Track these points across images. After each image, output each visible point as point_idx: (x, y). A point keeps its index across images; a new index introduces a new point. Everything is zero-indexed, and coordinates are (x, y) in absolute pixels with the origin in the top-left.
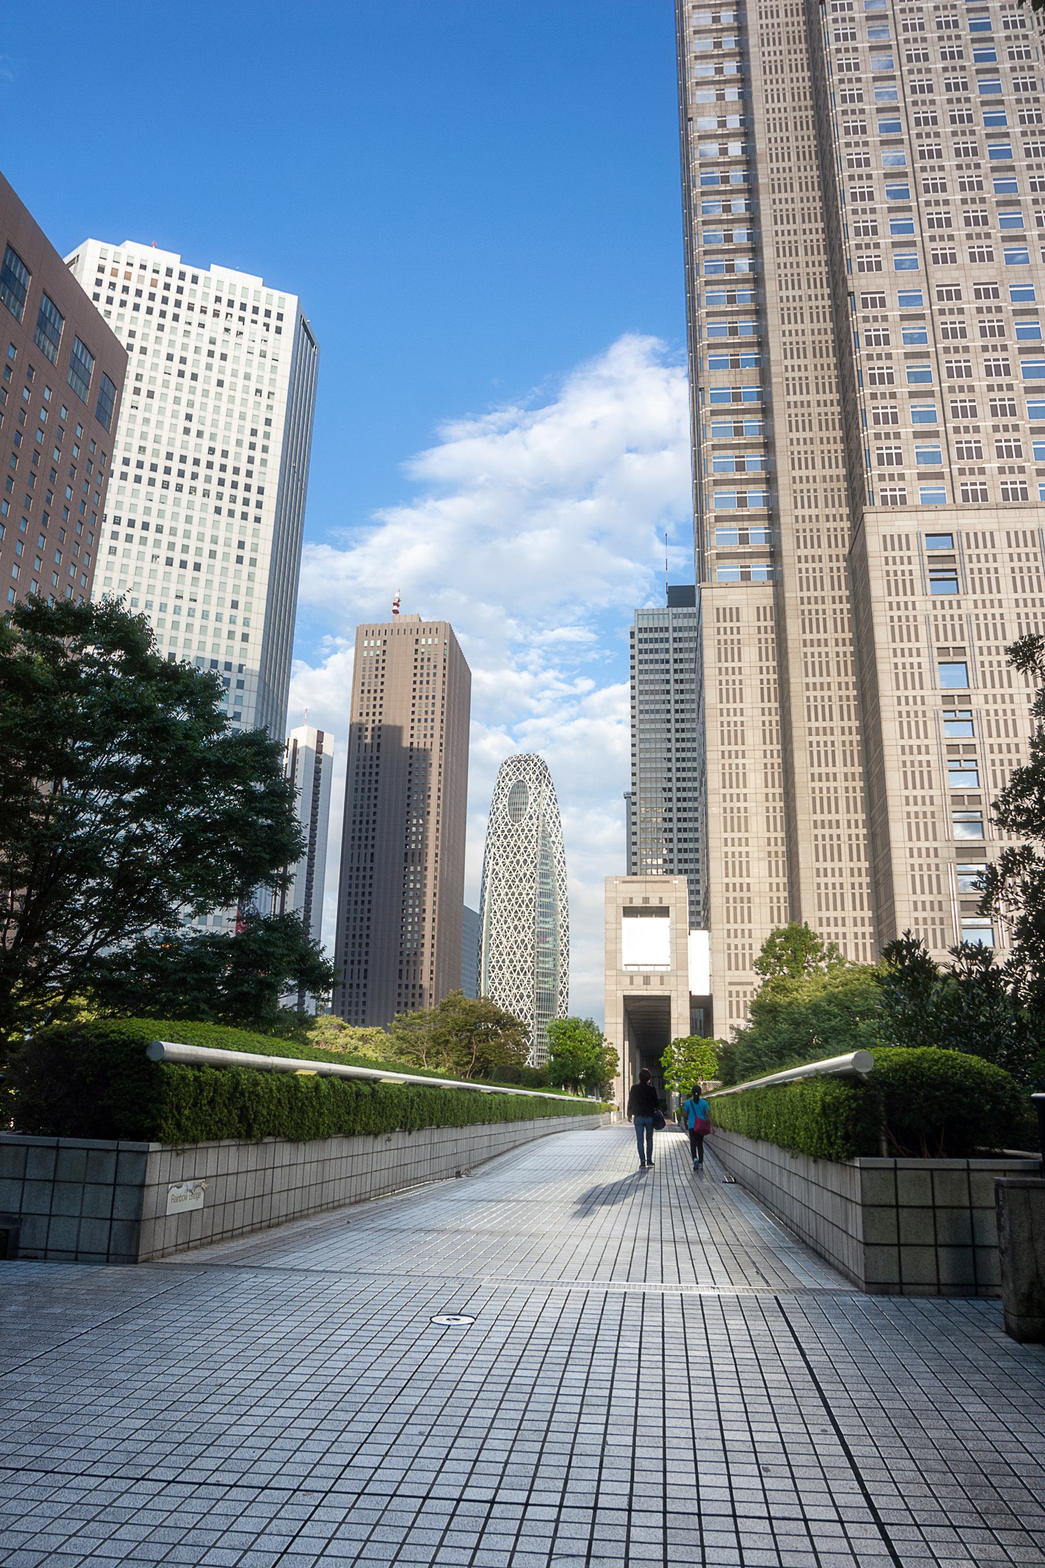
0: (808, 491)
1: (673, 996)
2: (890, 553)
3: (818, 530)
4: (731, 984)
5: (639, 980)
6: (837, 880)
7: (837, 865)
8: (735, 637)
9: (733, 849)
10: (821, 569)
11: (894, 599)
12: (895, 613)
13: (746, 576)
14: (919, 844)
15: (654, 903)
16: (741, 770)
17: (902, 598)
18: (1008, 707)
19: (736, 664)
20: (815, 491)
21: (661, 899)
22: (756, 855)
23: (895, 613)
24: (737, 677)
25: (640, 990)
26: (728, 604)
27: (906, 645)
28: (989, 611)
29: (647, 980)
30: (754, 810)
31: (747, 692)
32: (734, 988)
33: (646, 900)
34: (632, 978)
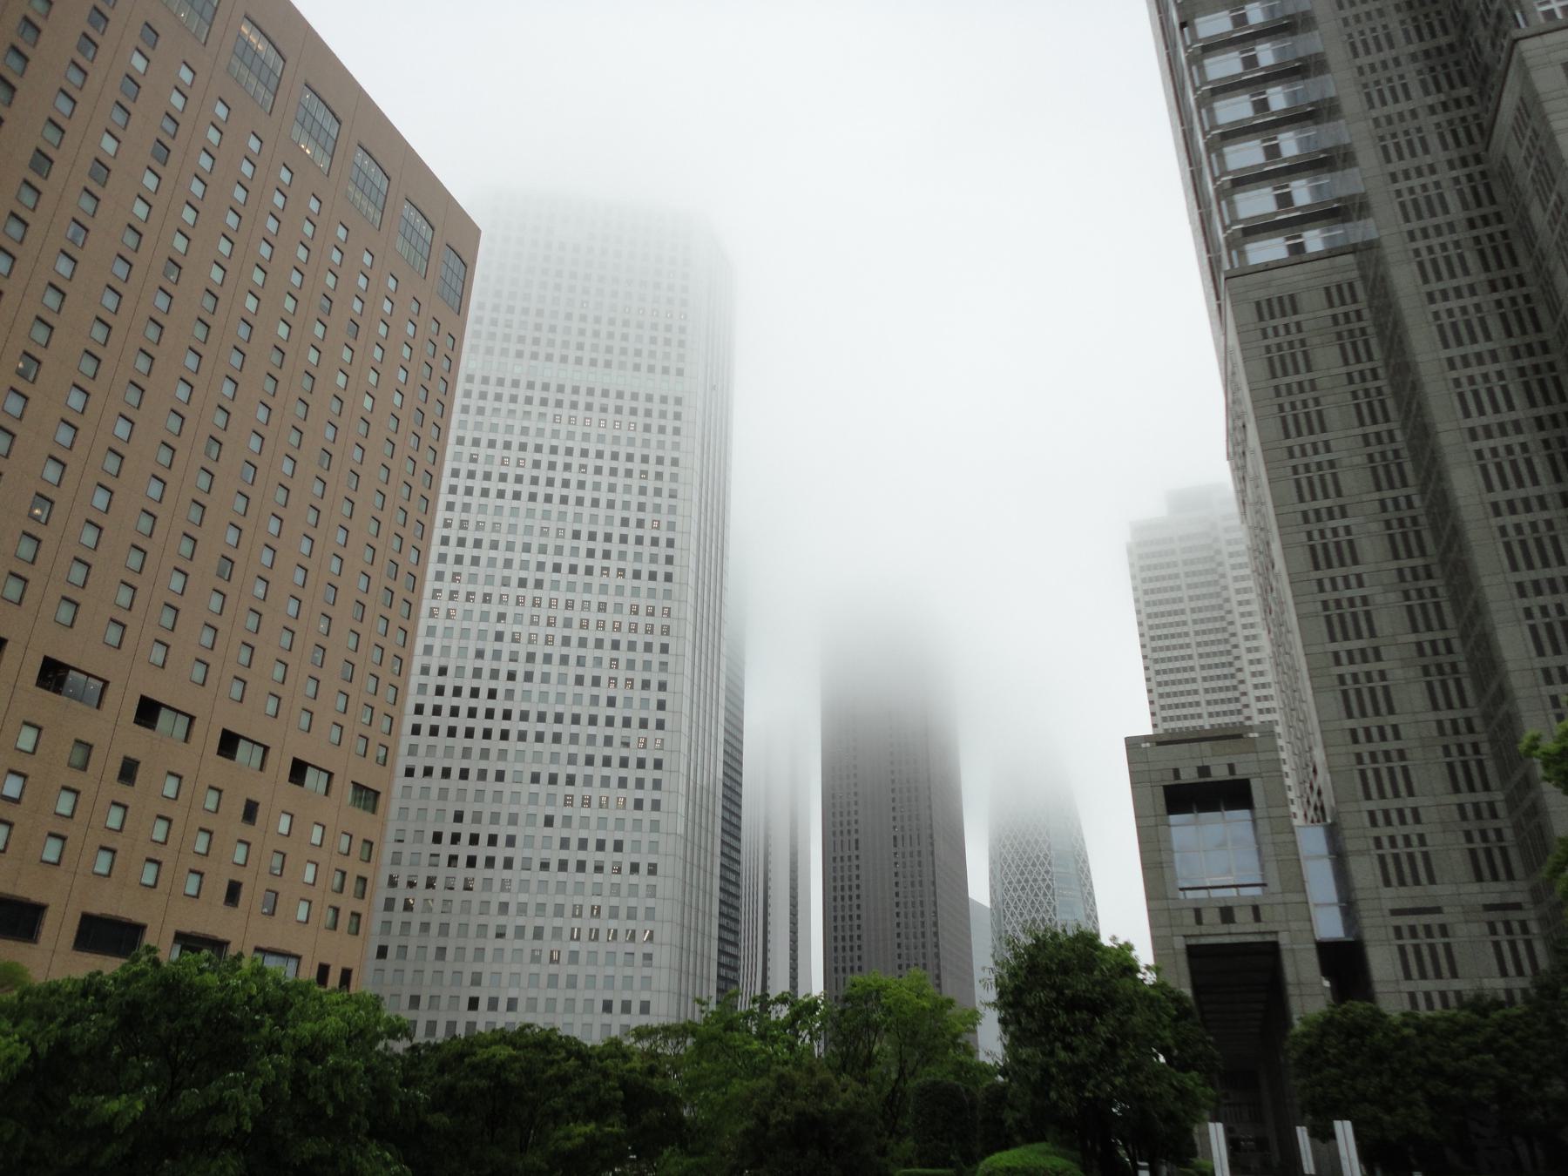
1: (1284, 940)
3: (1419, 130)
4: (1395, 912)
5: (1211, 917)
15: (1219, 773)
16: (1342, 536)
19: (1304, 376)
20: (1401, 77)
21: (1231, 768)
22: (1399, 673)
25: (1216, 933)
26: (1273, 292)
30: (1379, 599)
31: (1332, 416)
33: (1204, 771)
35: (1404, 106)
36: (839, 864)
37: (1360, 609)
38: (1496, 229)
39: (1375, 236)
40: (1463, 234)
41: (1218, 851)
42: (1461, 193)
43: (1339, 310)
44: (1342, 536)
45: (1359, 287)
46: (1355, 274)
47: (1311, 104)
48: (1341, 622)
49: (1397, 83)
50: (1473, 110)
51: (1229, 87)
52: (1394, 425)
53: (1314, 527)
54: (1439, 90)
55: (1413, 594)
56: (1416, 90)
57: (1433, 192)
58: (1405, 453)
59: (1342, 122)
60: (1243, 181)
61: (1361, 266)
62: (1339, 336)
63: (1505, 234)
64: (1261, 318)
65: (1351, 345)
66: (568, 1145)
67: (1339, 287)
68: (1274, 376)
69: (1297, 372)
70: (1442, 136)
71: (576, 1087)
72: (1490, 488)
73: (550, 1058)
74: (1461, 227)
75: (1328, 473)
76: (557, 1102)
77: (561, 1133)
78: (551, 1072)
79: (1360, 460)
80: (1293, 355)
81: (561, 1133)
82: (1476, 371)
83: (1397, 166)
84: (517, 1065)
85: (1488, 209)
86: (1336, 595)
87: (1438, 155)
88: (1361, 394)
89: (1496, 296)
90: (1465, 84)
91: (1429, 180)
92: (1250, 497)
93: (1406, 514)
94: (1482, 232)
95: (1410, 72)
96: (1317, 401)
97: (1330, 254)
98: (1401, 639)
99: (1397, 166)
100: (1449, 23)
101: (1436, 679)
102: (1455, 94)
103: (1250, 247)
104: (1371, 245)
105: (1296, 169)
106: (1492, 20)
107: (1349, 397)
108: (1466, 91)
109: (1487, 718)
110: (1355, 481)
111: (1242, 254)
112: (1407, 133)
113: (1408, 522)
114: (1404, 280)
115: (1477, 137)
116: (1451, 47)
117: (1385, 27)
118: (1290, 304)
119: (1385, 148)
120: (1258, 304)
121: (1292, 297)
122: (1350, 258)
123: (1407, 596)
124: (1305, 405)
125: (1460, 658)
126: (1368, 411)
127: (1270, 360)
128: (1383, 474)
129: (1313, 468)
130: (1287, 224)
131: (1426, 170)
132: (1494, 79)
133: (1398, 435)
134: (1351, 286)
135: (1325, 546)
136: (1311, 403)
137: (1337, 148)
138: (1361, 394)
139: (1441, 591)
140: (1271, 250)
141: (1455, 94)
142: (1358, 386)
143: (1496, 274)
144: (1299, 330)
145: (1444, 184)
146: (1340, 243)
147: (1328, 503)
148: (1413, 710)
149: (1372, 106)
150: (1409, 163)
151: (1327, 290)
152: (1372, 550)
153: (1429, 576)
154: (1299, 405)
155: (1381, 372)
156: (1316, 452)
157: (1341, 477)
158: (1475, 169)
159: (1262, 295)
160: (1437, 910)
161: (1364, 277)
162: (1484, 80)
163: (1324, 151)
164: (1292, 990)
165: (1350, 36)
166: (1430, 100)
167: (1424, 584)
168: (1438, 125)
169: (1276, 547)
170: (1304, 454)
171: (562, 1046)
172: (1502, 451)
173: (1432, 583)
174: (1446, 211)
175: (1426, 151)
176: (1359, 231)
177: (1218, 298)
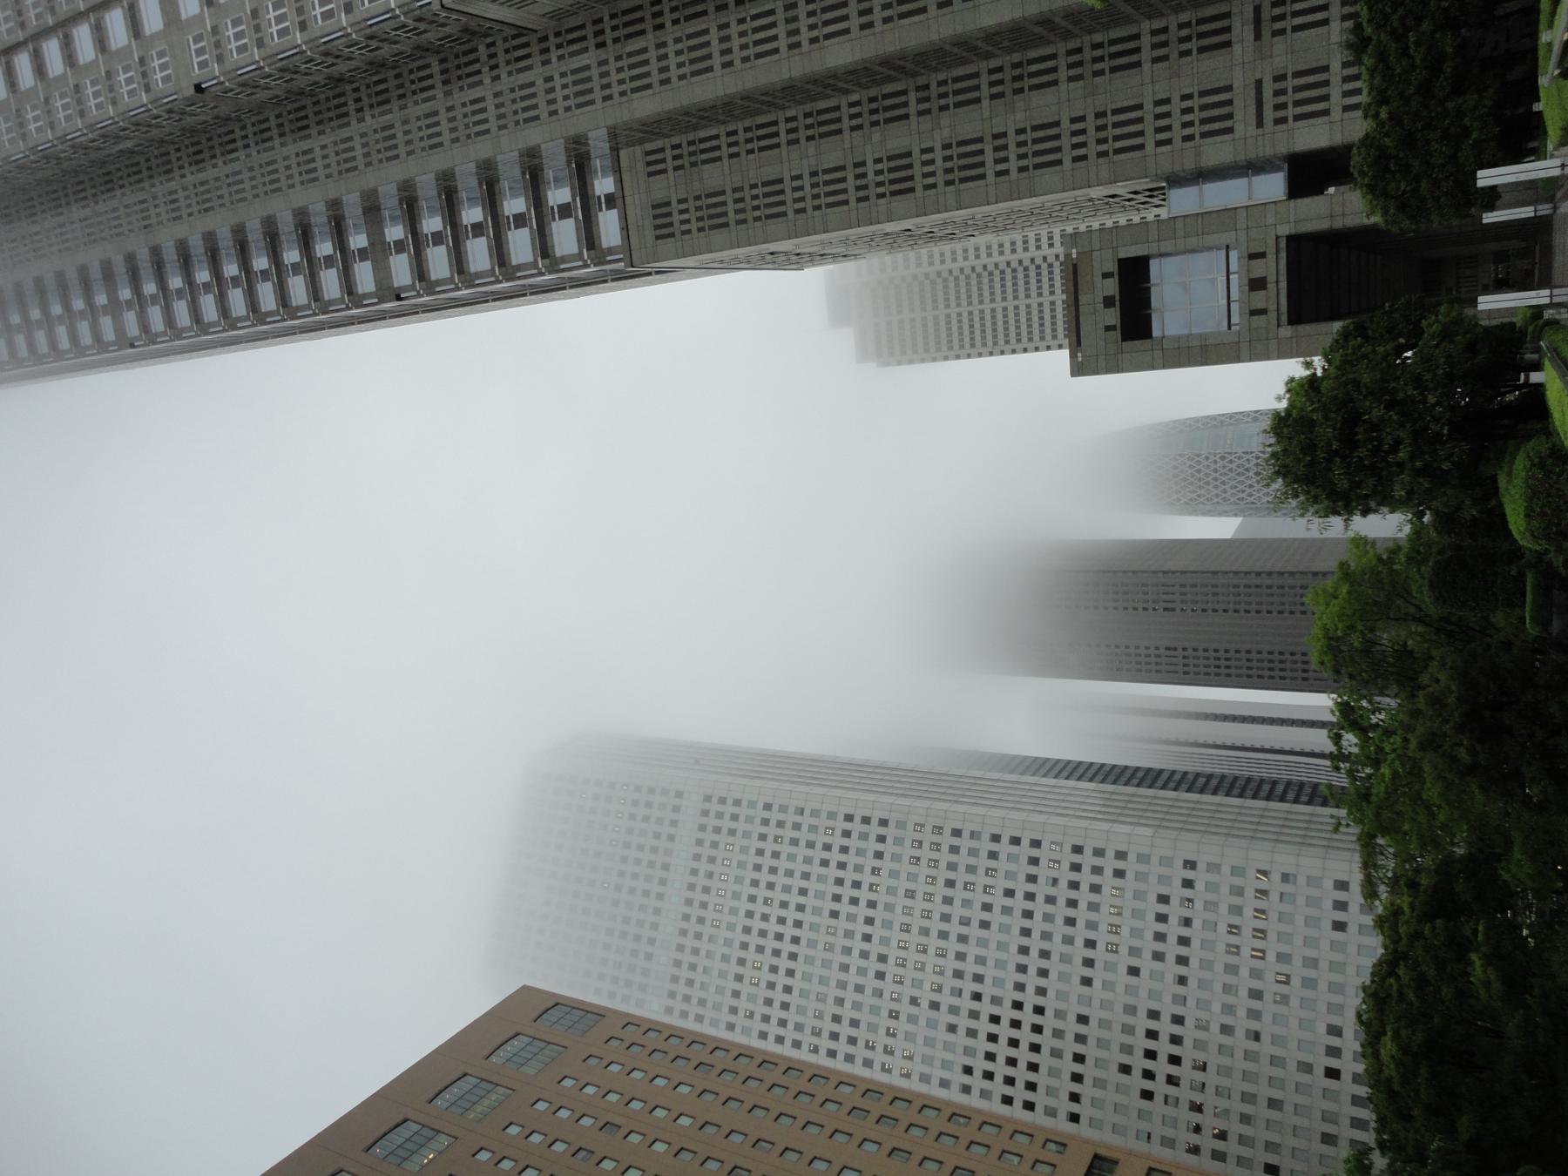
0: (465, 116)
1: (1285, 230)
3: (512, 90)
5: (1259, 299)
9: (1013, 157)
10: (563, 75)
15: (1111, 287)
19: (729, 198)
20: (464, 105)
21: (1106, 275)
22: (1020, 116)
24: (747, 193)
25: (1276, 296)
26: (649, 223)
30: (946, 133)
31: (769, 173)
32: (1269, 114)
33: (1108, 302)
34: (1253, 313)
35: (490, 103)
36: (1233, 671)
37: (955, 151)
38: (607, 24)
39: (604, 131)
40: (609, 53)
41: (1189, 290)
42: (572, 54)
43: (670, 164)
45: (649, 146)
46: (638, 149)
47: (480, 184)
48: (967, 168)
49: (469, 109)
50: (499, 43)
51: (458, 259)
52: (781, 116)
53: (873, 191)
54: (479, 72)
55: (943, 102)
56: (476, 93)
57: (569, 79)
58: (808, 107)
59: (499, 158)
60: (544, 247)
61: (631, 144)
62: (693, 164)
63: (612, 17)
64: (672, 235)
65: (707, 153)
66: (1497, 987)
67: (649, 164)
68: (726, 225)
69: (724, 204)
70: (520, 71)
71: (1430, 971)
72: (847, 31)
73: (1395, 995)
74: (603, 54)
75: (822, 178)
76: (1447, 992)
77: (1482, 992)
78: (1412, 997)
79: (811, 148)
80: (708, 207)
81: (1482, 992)
82: (736, 43)
83: (543, 111)
84: (1404, 1032)
85: (589, 31)
86: (940, 172)
87: (537, 74)
88: (749, 146)
89: (668, 24)
90: (475, 50)
91: (558, 82)
92: (841, 250)
93: (865, 108)
94: (609, 36)
95: (459, 97)
96: (754, 186)
97: (617, 170)
98: (986, 114)
99: (543, 111)
100: (420, 63)
101: (1027, 83)
102: (484, 58)
103: (605, 244)
104: (613, 134)
105: (538, 201)
106: (423, 26)
107: (751, 157)
108: (482, 48)
109: (1067, 35)
110: (832, 153)
111: (610, 251)
112: (514, 101)
113: (874, 106)
114: (646, 106)
115: (524, 40)
116: (442, 61)
117: (418, 119)
118: (661, 209)
119: (526, 121)
120: (658, 238)
121: (654, 207)
122: (622, 153)
123: (944, 108)
124: (755, 197)
125: (1007, 60)
126: (766, 140)
127: (712, 228)
128: (826, 127)
129: (816, 191)
130: (586, 209)
131: (549, 85)
132: (473, 24)
133: (790, 113)
134: (648, 153)
135: (892, 182)
136: (755, 192)
137: (522, 163)
138: (749, 146)
139: (941, 77)
140: (609, 225)
141: (484, 58)
143: (648, 25)
144: (685, 201)
145: (563, 69)
146: (608, 162)
147: (850, 178)
148: (1058, 103)
149: (487, 131)
150: (541, 100)
151: (650, 174)
152: (898, 138)
153: (927, 87)
154: (756, 203)
155: (730, 128)
156: (801, 188)
157: (826, 167)
158: (553, 41)
159: (650, 234)
160: (1259, 84)
161: (642, 141)
162: (474, 33)
163: (523, 174)
164: (1338, 224)
165: (423, 149)
166: (487, 81)
167: (934, 91)
168: (510, 73)
169: (889, 227)
170: (802, 199)
171: (1383, 980)
172: (812, 20)
173: (933, 85)
174: (588, 67)
175: (532, 84)
176: (599, 144)
177: (649, 274)
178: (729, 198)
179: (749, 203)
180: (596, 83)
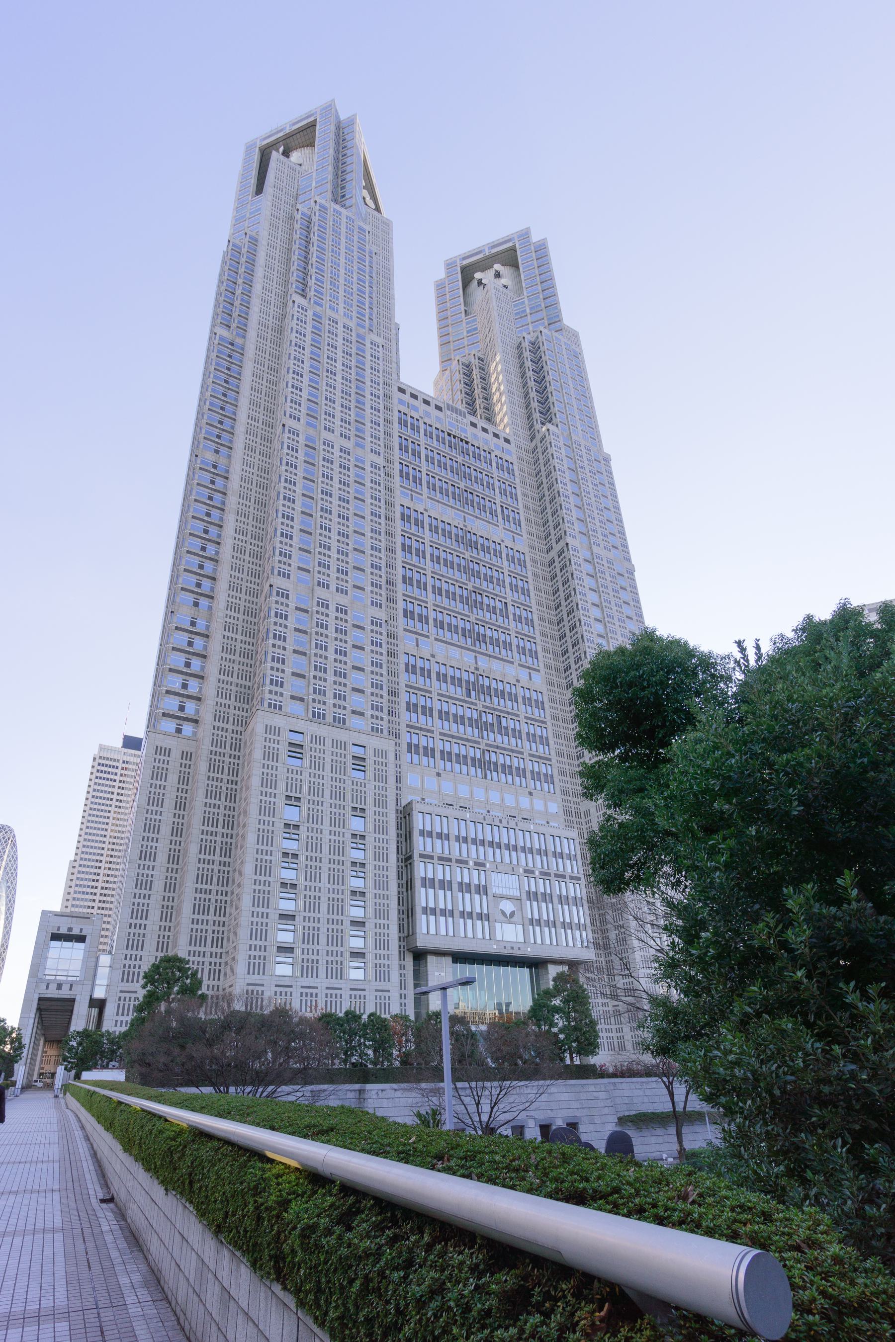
1: (77, 999)
2: (268, 736)
5: (53, 987)
6: (204, 927)
7: (205, 917)
8: (165, 766)
11: (266, 762)
12: (266, 771)
13: (179, 731)
14: (258, 909)
15: (76, 932)
16: (153, 850)
17: (270, 763)
18: (319, 836)
19: (163, 783)
23: (266, 771)
25: (52, 993)
27: (269, 790)
28: (317, 780)
29: (59, 987)
34: (48, 984)
37: (149, 879)
41: (67, 960)
44: (153, 850)
83: (217, 724)
99: (217, 724)
118: (168, 752)
142: (180, 794)
150: (221, 725)
159: (159, 744)
164: (74, 1017)
178: (163, 783)
179: (157, 791)
180: (218, 750)
